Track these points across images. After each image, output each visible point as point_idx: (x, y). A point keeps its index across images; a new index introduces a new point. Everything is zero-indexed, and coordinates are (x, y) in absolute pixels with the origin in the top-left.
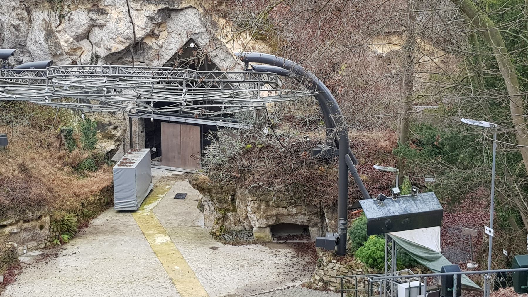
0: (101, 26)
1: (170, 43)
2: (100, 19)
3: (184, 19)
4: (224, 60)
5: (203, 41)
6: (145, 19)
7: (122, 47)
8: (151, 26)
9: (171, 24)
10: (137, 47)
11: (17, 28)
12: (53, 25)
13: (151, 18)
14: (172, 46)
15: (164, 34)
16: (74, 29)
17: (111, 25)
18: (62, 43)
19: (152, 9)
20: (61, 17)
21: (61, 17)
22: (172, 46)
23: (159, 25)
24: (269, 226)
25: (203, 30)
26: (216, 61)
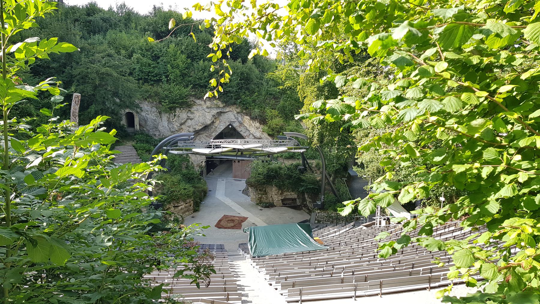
0: (191, 119)
1: (221, 126)
2: (191, 116)
3: (227, 116)
4: (245, 132)
5: (236, 125)
6: (211, 116)
7: (201, 128)
8: (213, 119)
9: (221, 118)
10: (206, 128)
11: (155, 120)
12: (171, 119)
13: (214, 116)
14: (221, 127)
15: (218, 122)
16: (180, 120)
17: (196, 119)
18: (175, 127)
19: (215, 111)
20: (175, 115)
21: (175, 115)
22: (221, 127)
23: (216, 118)
24: (281, 200)
25: (236, 120)
26: (241, 133)
